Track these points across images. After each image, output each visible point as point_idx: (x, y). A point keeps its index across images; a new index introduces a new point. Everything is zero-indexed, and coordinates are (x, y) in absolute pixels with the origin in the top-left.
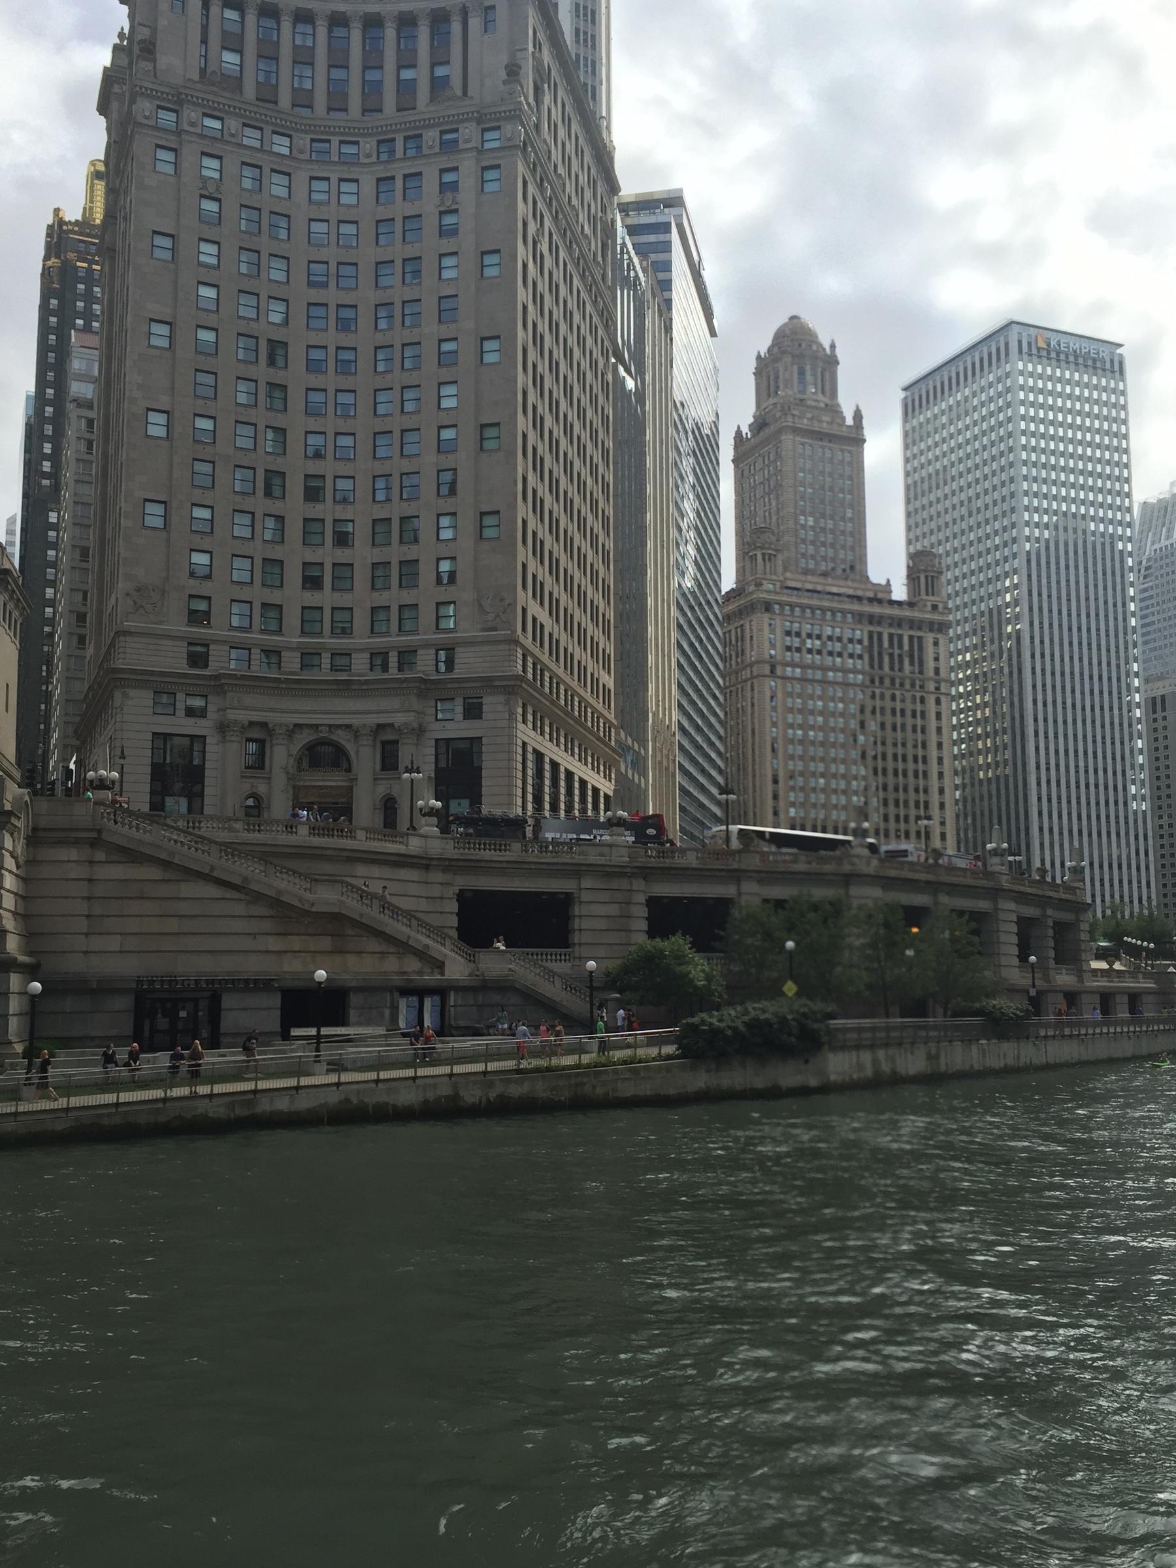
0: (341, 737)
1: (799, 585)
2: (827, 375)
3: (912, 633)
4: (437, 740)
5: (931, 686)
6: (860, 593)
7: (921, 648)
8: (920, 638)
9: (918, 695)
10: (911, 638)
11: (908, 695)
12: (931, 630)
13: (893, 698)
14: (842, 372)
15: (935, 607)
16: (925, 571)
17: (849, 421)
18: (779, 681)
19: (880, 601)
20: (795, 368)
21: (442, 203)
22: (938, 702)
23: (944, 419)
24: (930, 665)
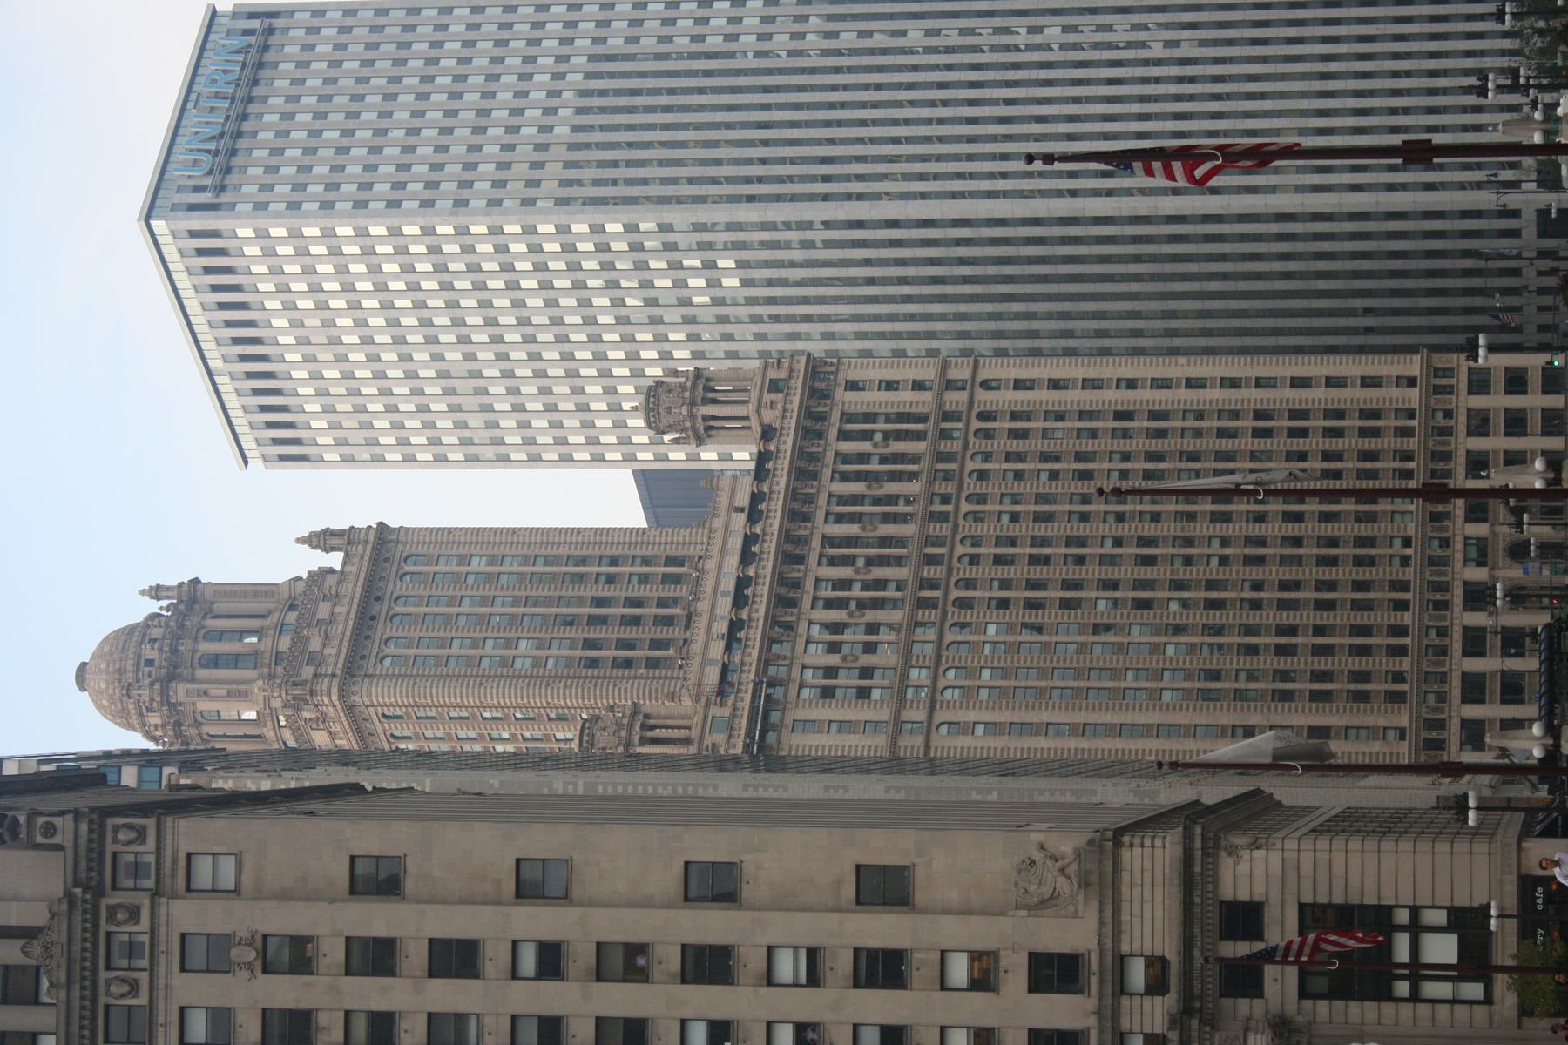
1: (713, 676)
2: (221, 607)
3: (833, 433)
4: (1303, 993)
5: (956, 398)
6: (736, 543)
7: (870, 417)
8: (847, 417)
9: (976, 424)
10: (844, 435)
11: (976, 444)
12: (826, 395)
13: (982, 475)
14: (214, 574)
15: (775, 386)
16: (693, 403)
17: (335, 560)
18: (940, 716)
19: (756, 498)
20: (201, 673)
21: (249, 966)
22: (986, 385)
23: (331, 373)
24: (906, 398)
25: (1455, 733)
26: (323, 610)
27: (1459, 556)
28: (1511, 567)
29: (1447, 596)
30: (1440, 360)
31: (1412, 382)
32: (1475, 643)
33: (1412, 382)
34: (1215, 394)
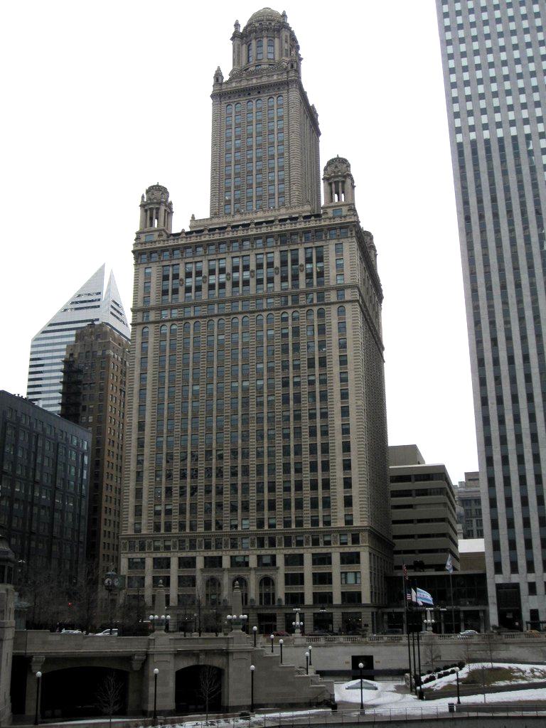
25: (137, 556)
27: (184, 555)
28: (229, 579)
29: (213, 549)
31: (349, 522)
32: (187, 563)
33: (349, 522)
34: (337, 421)
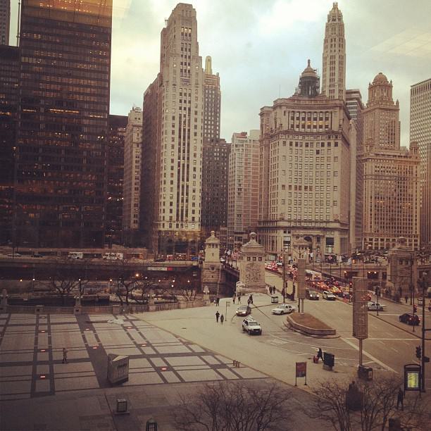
0: (311, 236)
15: (417, 158)
26: (388, 104)
30: (419, 237)
31: (416, 232)
